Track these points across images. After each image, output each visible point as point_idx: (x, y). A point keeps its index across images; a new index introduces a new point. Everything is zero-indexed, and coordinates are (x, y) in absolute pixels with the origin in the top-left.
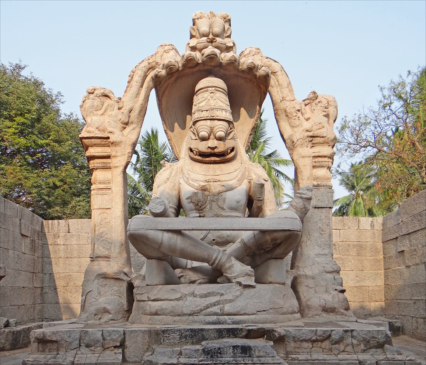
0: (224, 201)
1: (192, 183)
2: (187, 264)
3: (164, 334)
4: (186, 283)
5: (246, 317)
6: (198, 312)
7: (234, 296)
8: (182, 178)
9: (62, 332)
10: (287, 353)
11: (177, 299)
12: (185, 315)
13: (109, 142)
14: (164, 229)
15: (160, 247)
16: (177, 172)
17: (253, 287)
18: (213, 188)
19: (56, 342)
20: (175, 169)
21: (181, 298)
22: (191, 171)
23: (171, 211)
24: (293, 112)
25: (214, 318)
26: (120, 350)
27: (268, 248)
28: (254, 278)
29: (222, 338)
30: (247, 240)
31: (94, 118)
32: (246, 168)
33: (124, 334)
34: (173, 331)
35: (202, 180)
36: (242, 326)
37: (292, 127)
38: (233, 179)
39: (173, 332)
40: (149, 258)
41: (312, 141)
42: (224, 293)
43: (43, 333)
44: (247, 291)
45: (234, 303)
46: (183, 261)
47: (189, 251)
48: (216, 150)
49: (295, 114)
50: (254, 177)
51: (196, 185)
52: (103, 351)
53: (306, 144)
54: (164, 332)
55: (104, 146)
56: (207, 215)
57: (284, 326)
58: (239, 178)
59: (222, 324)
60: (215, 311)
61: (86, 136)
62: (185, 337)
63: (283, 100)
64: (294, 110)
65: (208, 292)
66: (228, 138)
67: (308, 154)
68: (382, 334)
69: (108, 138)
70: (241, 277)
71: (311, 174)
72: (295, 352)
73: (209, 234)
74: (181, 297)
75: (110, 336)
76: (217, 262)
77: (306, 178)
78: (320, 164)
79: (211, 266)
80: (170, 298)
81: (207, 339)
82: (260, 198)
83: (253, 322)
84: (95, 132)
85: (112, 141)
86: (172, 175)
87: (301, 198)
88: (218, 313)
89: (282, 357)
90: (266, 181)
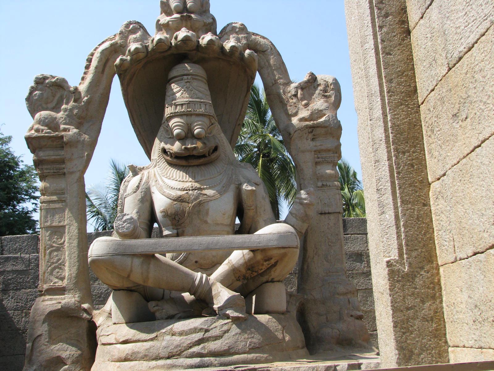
0: (207, 213)
4: (162, 319)
5: (236, 357)
6: (177, 353)
7: (221, 331)
8: (154, 186)
13: (63, 142)
14: (133, 253)
15: (129, 276)
23: (141, 231)
27: (261, 270)
32: (232, 169)
36: (231, 368)
41: (312, 132)
48: (195, 153)
50: (242, 180)
55: (56, 147)
58: (224, 184)
60: (199, 351)
61: (33, 136)
63: (275, 84)
64: (289, 95)
65: (189, 328)
66: (209, 135)
69: (62, 137)
73: (190, 255)
76: (199, 291)
78: (324, 160)
79: (193, 296)
82: (251, 206)
84: (44, 131)
86: (143, 183)
88: (202, 353)
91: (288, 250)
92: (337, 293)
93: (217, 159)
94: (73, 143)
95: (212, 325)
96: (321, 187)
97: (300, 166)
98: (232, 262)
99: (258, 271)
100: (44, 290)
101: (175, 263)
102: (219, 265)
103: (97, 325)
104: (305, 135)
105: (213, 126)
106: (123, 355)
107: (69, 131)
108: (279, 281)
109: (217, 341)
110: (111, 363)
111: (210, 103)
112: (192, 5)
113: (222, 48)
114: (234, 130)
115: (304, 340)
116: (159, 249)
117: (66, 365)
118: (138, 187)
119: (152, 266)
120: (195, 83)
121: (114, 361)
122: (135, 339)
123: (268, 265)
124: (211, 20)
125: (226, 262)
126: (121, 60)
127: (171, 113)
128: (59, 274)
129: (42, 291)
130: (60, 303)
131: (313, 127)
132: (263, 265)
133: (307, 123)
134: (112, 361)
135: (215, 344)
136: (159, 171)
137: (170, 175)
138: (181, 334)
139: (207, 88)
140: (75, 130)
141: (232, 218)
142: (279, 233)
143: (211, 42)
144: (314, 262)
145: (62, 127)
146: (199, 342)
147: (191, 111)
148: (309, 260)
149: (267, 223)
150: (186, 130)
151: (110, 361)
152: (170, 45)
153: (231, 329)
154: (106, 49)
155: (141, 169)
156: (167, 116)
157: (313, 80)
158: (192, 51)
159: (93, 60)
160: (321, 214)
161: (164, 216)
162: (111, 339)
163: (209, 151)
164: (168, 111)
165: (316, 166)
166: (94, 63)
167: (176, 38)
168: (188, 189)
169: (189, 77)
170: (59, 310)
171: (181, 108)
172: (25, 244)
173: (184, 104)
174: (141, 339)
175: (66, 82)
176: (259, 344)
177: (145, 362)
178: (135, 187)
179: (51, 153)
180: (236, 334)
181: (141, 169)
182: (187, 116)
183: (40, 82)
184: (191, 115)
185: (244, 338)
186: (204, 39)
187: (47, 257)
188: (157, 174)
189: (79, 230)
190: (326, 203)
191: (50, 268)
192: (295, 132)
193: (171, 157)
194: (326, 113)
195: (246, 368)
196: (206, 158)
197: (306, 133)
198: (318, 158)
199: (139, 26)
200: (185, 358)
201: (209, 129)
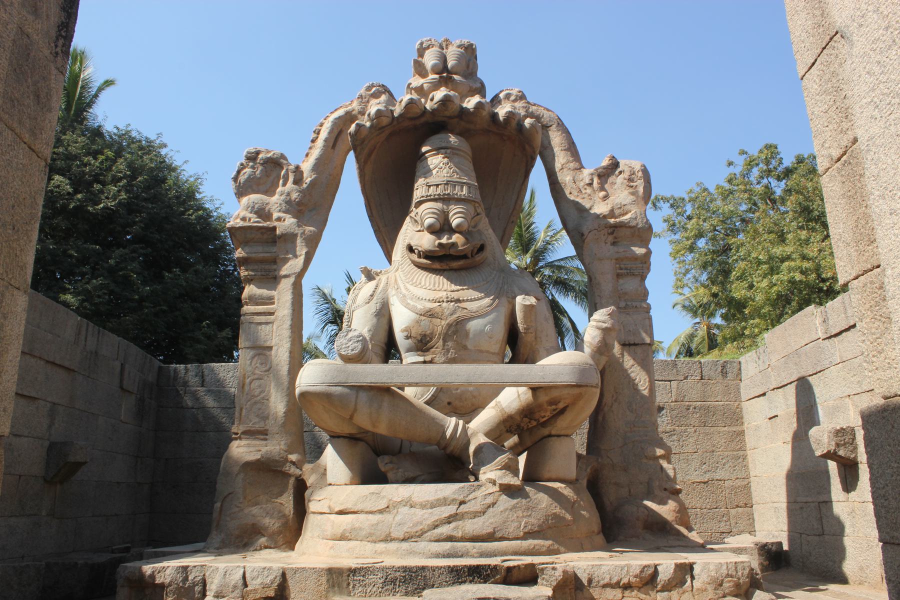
1: (412, 303)
2: (401, 445)
6: (417, 534)
8: (394, 295)
11: (381, 512)
12: (392, 540)
15: (351, 417)
20: (383, 279)
21: (388, 510)
22: (410, 283)
24: (581, 187)
27: (543, 418)
29: (461, 583)
30: (506, 404)
33: (284, 575)
35: (427, 299)
39: (371, 572)
45: (483, 517)
48: (452, 252)
51: (419, 307)
54: (353, 571)
55: (267, 242)
56: (436, 359)
59: (462, 556)
61: (238, 226)
62: (393, 581)
64: (582, 184)
65: (437, 497)
66: (473, 230)
69: (274, 228)
70: (496, 470)
74: (388, 507)
78: (628, 271)
79: (443, 451)
80: (368, 509)
81: (433, 586)
84: (252, 220)
85: (280, 234)
91: (584, 389)
92: (646, 456)
94: (289, 238)
95: (471, 496)
96: (625, 308)
97: (595, 278)
98: (501, 405)
99: (538, 419)
100: (240, 432)
101: (420, 402)
102: (481, 409)
103: (308, 485)
104: (603, 236)
105: (478, 216)
106: (339, 531)
107: (284, 220)
108: (567, 436)
109: (476, 520)
110: (321, 540)
111: (476, 186)
112: (456, 64)
113: (495, 116)
114: (505, 228)
117: (264, 536)
119: (385, 404)
123: (554, 410)
124: (479, 85)
125: (493, 404)
126: (357, 124)
127: (423, 197)
128: (261, 411)
129: (238, 434)
130: (260, 451)
132: (546, 411)
134: (323, 539)
135: (473, 524)
136: (402, 276)
137: (417, 281)
138: (423, 506)
139: (472, 167)
140: (294, 220)
141: (502, 344)
142: (571, 364)
143: (479, 106)
144: (612, 411)
145: (275, 215)
146: (449, 520)
147: (449, 194)
148: (606, 409)
149: (549, 353)
150: (442, 221)
151: (321, 537)
152: (424, 109)
153: (498, 502)
154: (340, 118)
155: (377, 274)
156: (417, 201)
157: (614, 165)
158: (453, 118)
159: (322, 132)
161: (407, 338)
163: (472, 251)
165: (617, 281)
166: (324, 134)
167: (432, 100)
168: (441, 300)
169: (449, 151)
170: (258, 460)
171: (435, 190)
172: (231, 374)
173: (440, 184)
174: (365, 510)
175: (285, 159)
176: (539, 526)
177: (369, 543)
178: (368, 295)
179: (260, 249)
180: (506, 510)
181: (377, 274)
182: (443, 201)
183: (252, 157)
185: (517, 517)
186: (470, 103)
188: (398, 279)
189: (290, 352)
190: (631, 330)
191: (249, 403)
192: (590, 232)
193: (419, 257)
194: (632, 209)
195: (520, 563)
196: (467, 260)
197: (604, 235)
199: (385, 90)
200: (427, 541)
201: (472, 218)
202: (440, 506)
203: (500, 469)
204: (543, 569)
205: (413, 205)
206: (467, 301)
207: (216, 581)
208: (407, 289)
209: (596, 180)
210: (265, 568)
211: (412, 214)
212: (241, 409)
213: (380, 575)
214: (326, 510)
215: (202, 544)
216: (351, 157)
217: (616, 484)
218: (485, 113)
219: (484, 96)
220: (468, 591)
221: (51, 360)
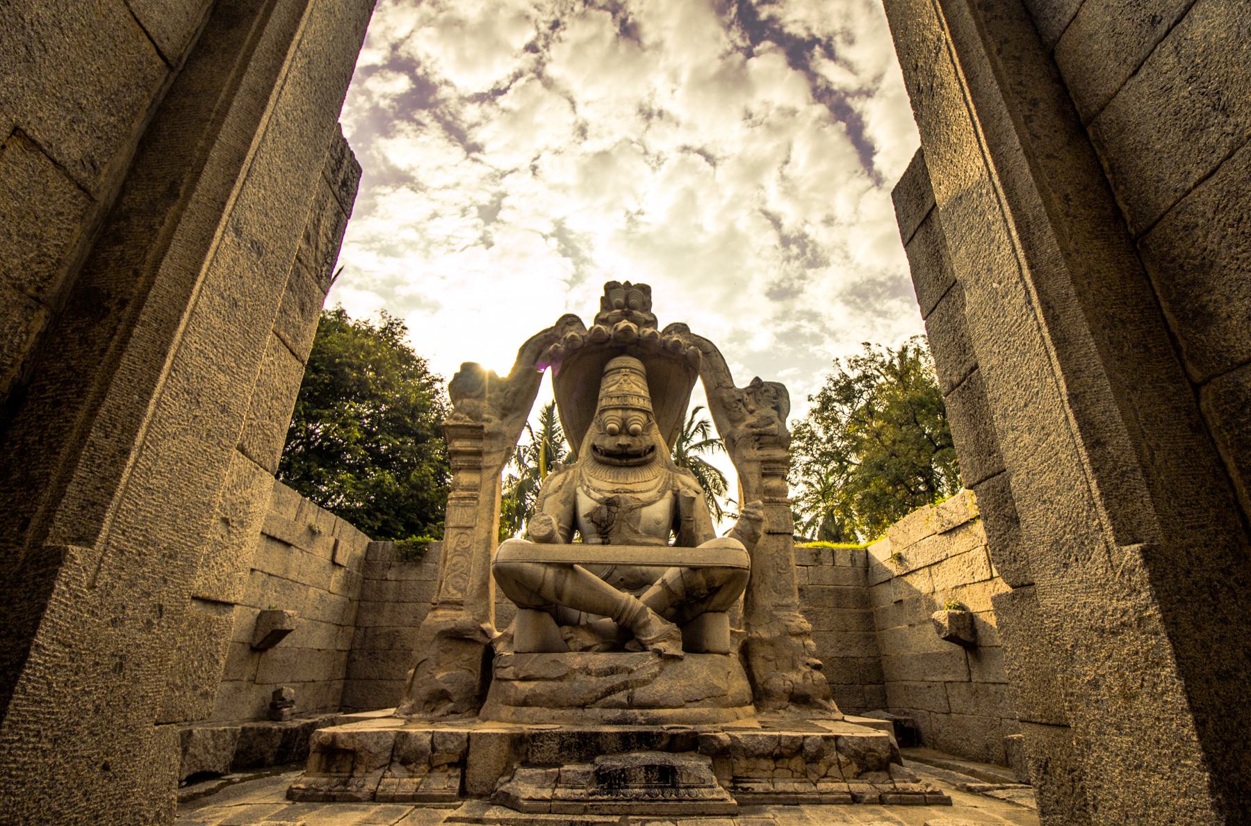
3: (534, 741)
4: (575, 650)
5: (667, 712)
9: (365, 733)
10: (735, 780)
11: (560, 679)
12: (571, 706)
15: (540, 590)
16: (573, 477)
17: (680, 659)
18: (622, 501)
19: (353, 753)
25: (618, 713)
26: (458, 772)
28: (681, 644)
31: (466, 401)
34: (550, 736)
37: (733, 422)
38: (653, 489)
40: (522, 606)
42: (635, 669)
43: (334, 736)
44: (669, 667)
46: (574, 613)
47: (583, 597)
48: (629, 450)
49: (734, 405)
50: (680, 486)
52: (430, 771)
53: (751, 444)
54: (534, 736)
57: (729, 729)
59: (631, 723)
62: (569, 748)
67: (755, 457)
68: (883, 743)
69: (482, 427)
71: (760, 485)
72: (748, 777)
74: (567, 674)
75: (444, 743)
76: (624, 616)
77: (754, 490)
81: (603, 753)
83: (679, 721)
87: (748, 518)
89: (725, 788)
90: (698, 493)
93: (651, 461)
115: (750, 691)
116: (582, 559)
117: (452, 701)
118: (560, 487)
120: (633, 377)
121: (510, 705)
122: (538, 675)
125: (659, 581)
131: (760, 435)
133: (754, 430)
143: (653, 335)
154: (540, 340)
160: (769, 533)
162: (508, 672)
164: (603, 403)
167: (616, 329)
177: (548, 710)
184: (627, 409)
187: (448, 564)
193: (602, 454)
195: (682, 731)
198: (765, 469)
201: (647, 427)
202: (612, 673)
203: (665, 641)
204: (703, 737)
205: (597, 412)
206: (641, 492)
207: (404, 747)
208: (589, 481)
209: (745, 396)
210: (452, 733)
211: (597, 420)
212: (441, 582)
213: (557, 740)
214: (511, 676)
215: (391, 711)
216: (548, 375)
217: (763, 657)
218: (658, 341)
219: (656, 328)
220: (636, 758)
221: (272, 534)
